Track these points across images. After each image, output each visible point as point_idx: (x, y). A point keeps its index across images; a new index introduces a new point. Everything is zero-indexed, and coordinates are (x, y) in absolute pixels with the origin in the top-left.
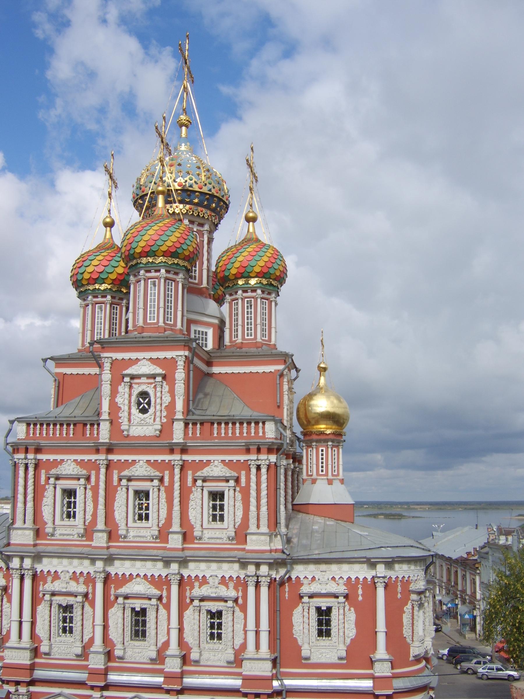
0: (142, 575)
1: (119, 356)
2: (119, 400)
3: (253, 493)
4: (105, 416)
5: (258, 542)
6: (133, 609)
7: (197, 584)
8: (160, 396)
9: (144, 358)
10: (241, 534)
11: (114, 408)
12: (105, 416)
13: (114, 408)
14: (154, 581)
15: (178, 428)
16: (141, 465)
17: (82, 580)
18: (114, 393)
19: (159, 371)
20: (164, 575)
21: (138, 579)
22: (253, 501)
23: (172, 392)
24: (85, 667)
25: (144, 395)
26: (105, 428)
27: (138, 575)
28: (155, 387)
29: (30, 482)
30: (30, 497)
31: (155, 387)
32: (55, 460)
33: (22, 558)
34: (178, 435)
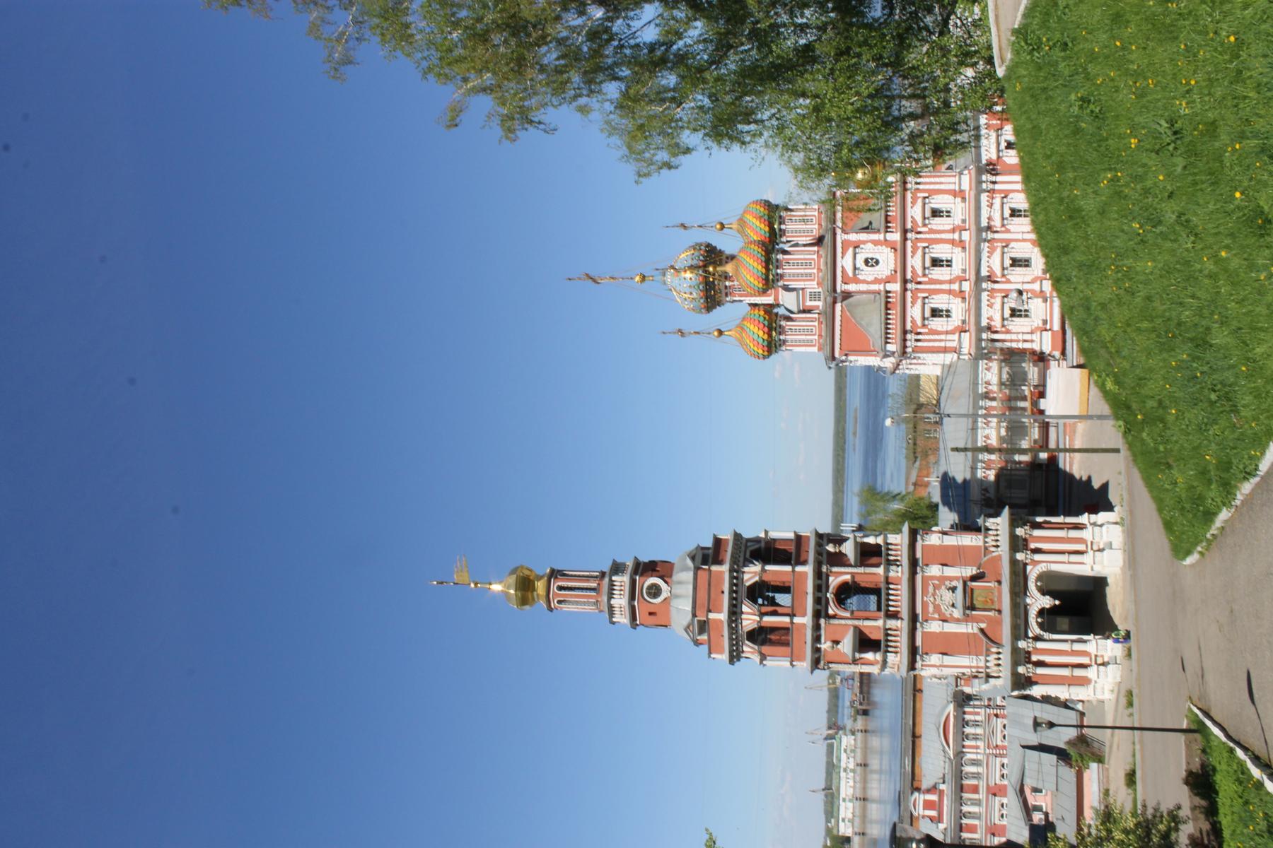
2: (870, 278)
3: (932, 187)
4: (881, 287)
5: (966, 182)
8: (868, 251)
10: (958, 194)
11: (876, 281)
12: (881, 287)
13: (876, 281)
15: (890, 237)
16: (915, 262)
18: (865, 282)
19: (851, 250)
22: (937, 187)
23: (864, 242)
24: (1051, 297)
25: (866, 262)
26: (889, 287)
34: (896, 237)
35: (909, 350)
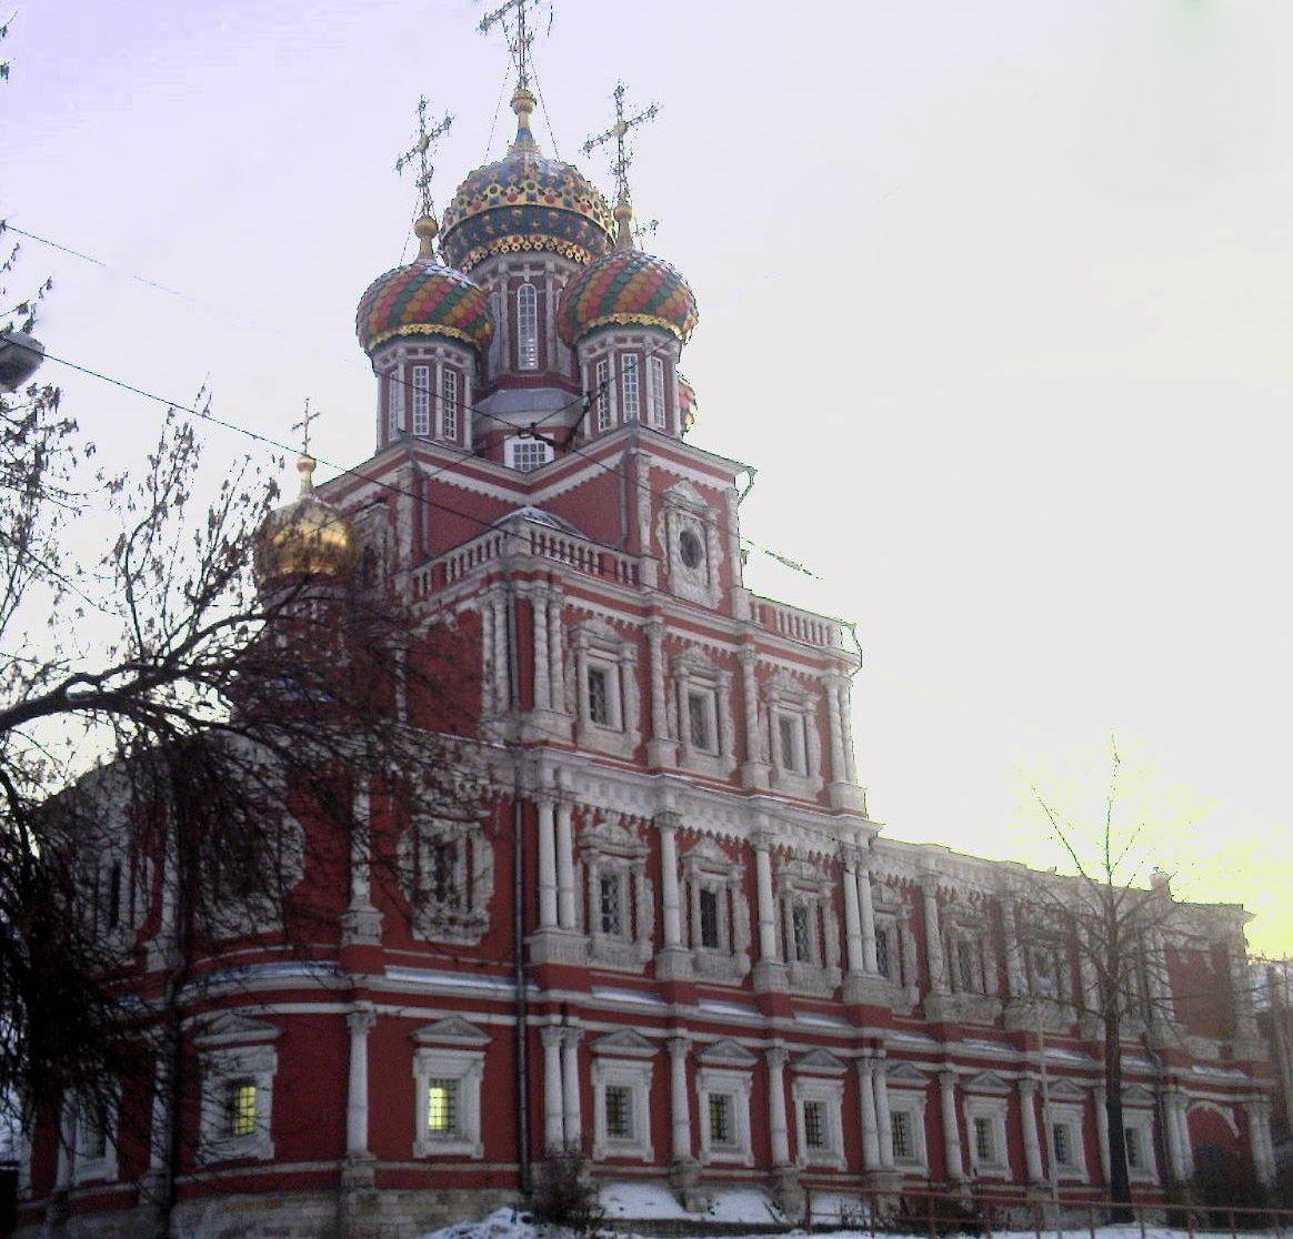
0: (714, 833)
1: (657, 460)
2: (660, 534)
6: (704, 893)
7: (782, 859)
9: (687, 479)
14: (725, 844)
17: (634, 828)
20: (742, 838)
21: (708, 839)
27: (709, 834)
28: (706, 530)
29: (557, 639)
30: (558, 667)
31: (706, 530)
32: (581, 609)
33: (556, 773)
35: (522, 584)
